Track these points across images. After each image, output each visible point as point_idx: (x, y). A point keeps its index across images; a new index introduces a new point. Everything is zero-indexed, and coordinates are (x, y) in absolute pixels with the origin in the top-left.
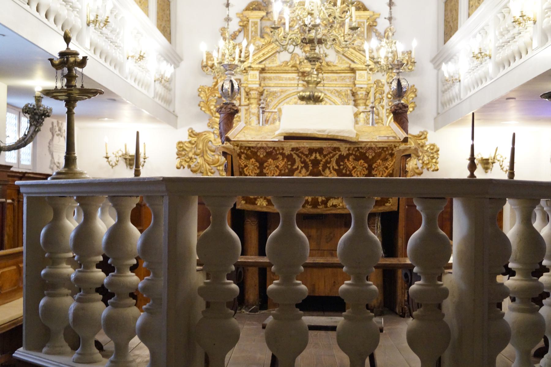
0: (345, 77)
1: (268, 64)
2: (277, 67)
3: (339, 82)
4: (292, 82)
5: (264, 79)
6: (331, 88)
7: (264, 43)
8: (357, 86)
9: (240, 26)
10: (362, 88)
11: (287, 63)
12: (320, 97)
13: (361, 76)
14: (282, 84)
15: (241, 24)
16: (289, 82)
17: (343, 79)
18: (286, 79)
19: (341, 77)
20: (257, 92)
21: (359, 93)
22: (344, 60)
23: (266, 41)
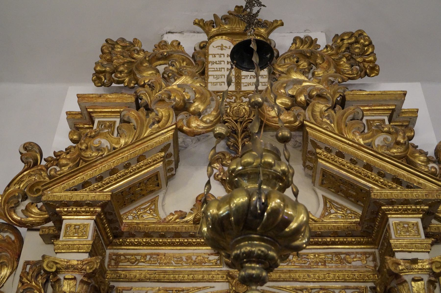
0: (347, 254)
1: (129, 217)
2: (154, 223)
3: (332, 266)
4: (196, 268)
5: (117, 259)
6: (311, 285)
7: (116, 146)
8: (398, 256)
9: (72, 140)
10: (415, 261)
11: (182, 215)
12: (287, 222)
13: (406, 228)
14: (165, 272)
15: (75, 137)
16: (186, 268)
17: (341, 261)
18: (179, 260)
19: (337, 254)
20: (80, 277)
21: (407, 277)
22: (342, 208)
23: (123, 141)
